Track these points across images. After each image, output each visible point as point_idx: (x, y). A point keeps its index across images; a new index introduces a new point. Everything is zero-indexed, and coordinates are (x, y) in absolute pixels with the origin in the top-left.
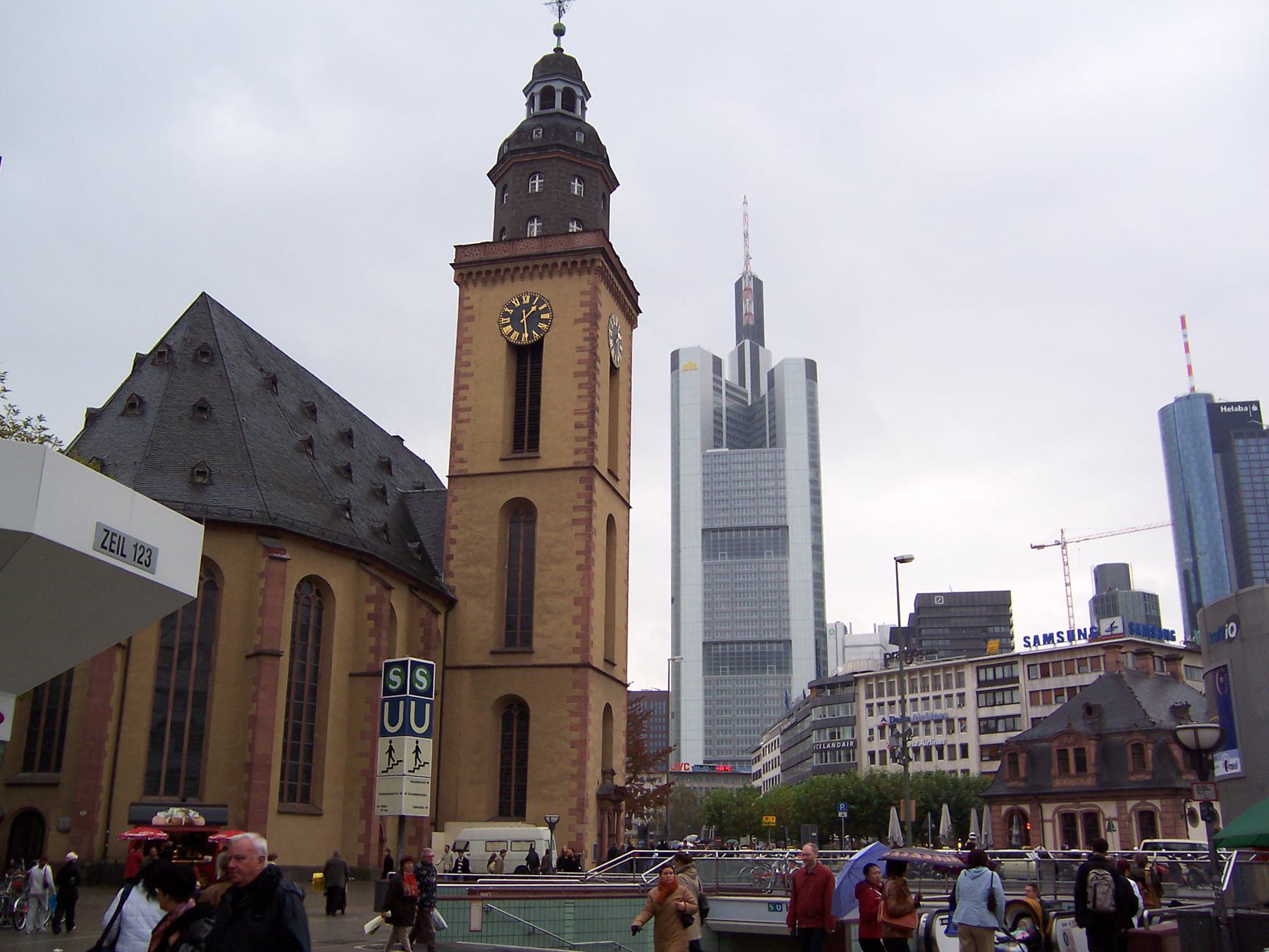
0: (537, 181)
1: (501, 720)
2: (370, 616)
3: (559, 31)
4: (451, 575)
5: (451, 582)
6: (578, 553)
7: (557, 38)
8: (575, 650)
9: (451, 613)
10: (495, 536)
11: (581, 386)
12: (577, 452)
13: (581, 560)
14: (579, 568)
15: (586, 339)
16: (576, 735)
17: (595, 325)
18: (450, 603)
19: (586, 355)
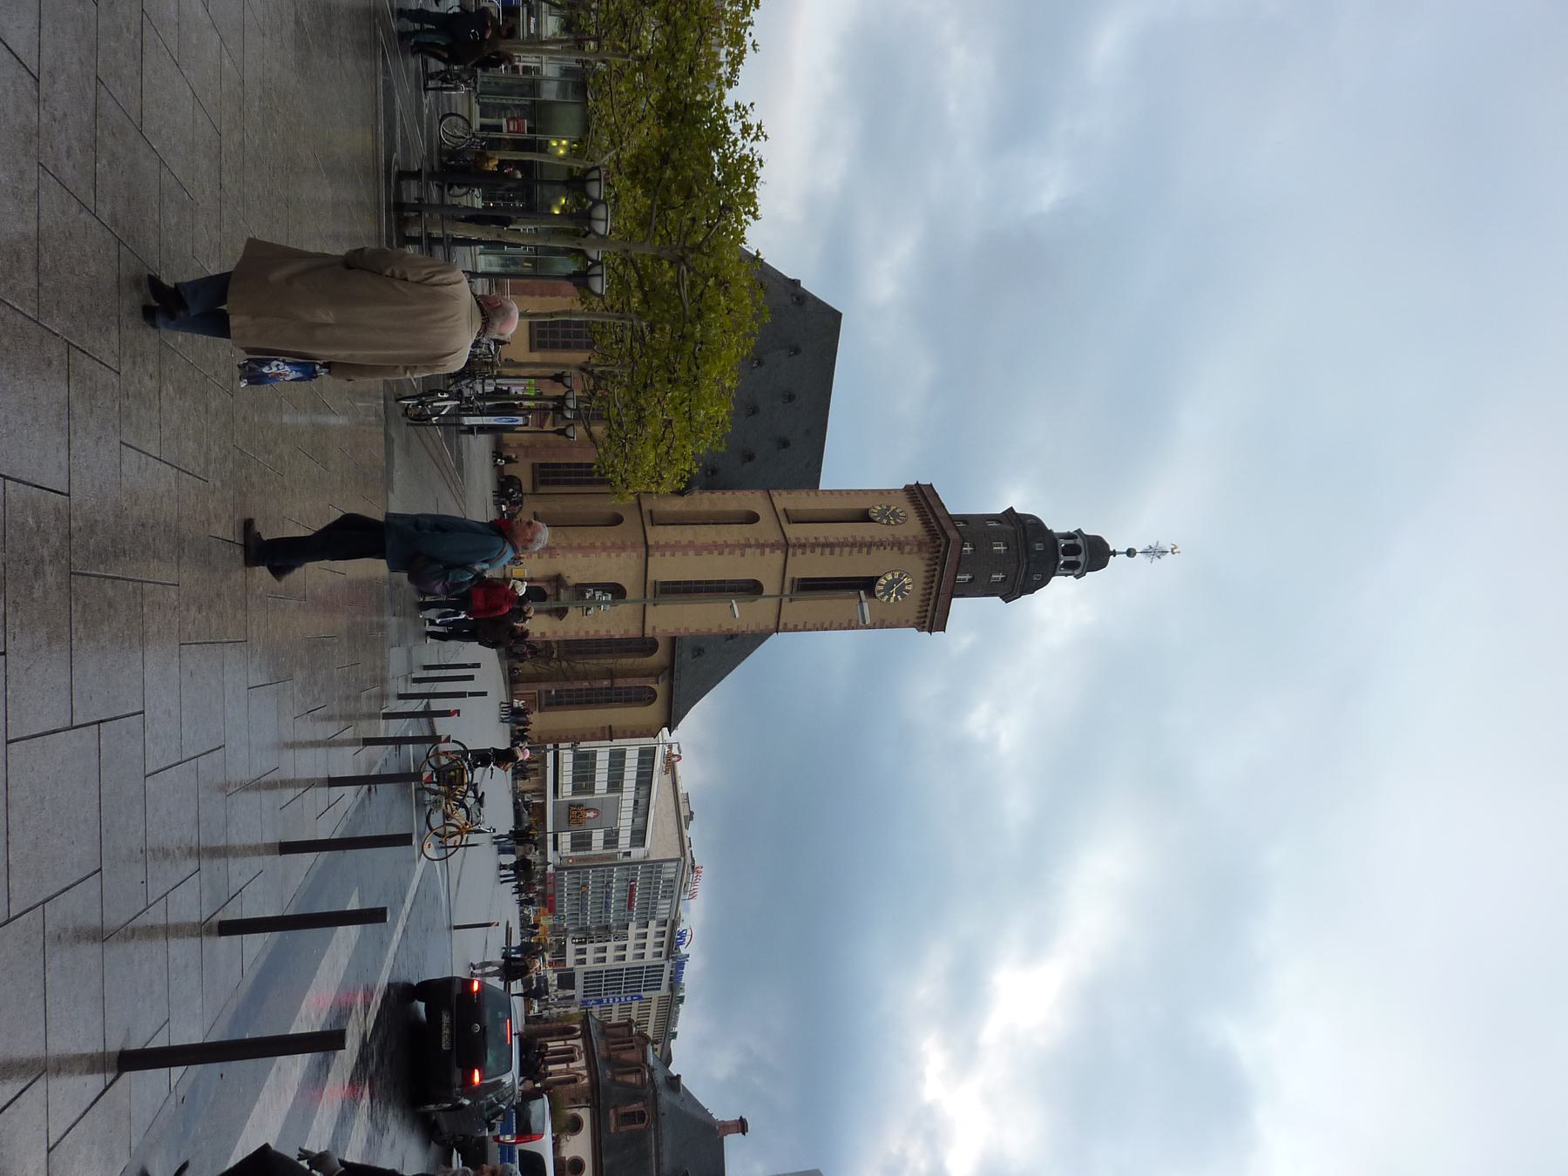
3: (1131, 553)
7: (1125, 551)
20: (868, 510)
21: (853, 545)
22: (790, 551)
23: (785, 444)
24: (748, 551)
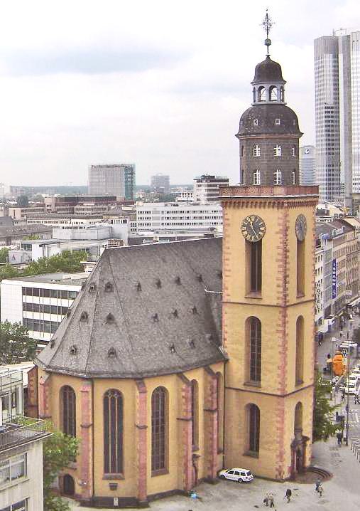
2: (183, 397)
4: (226, 347)
6: (279, 346)
10: (243, 332)
11: (279, 266)
12: (278, 298)
15: (281, 243)
16: (279, 425)
18: (226, 361)
20: (246, 240)
22: (287, 304)
24: (286, 332)
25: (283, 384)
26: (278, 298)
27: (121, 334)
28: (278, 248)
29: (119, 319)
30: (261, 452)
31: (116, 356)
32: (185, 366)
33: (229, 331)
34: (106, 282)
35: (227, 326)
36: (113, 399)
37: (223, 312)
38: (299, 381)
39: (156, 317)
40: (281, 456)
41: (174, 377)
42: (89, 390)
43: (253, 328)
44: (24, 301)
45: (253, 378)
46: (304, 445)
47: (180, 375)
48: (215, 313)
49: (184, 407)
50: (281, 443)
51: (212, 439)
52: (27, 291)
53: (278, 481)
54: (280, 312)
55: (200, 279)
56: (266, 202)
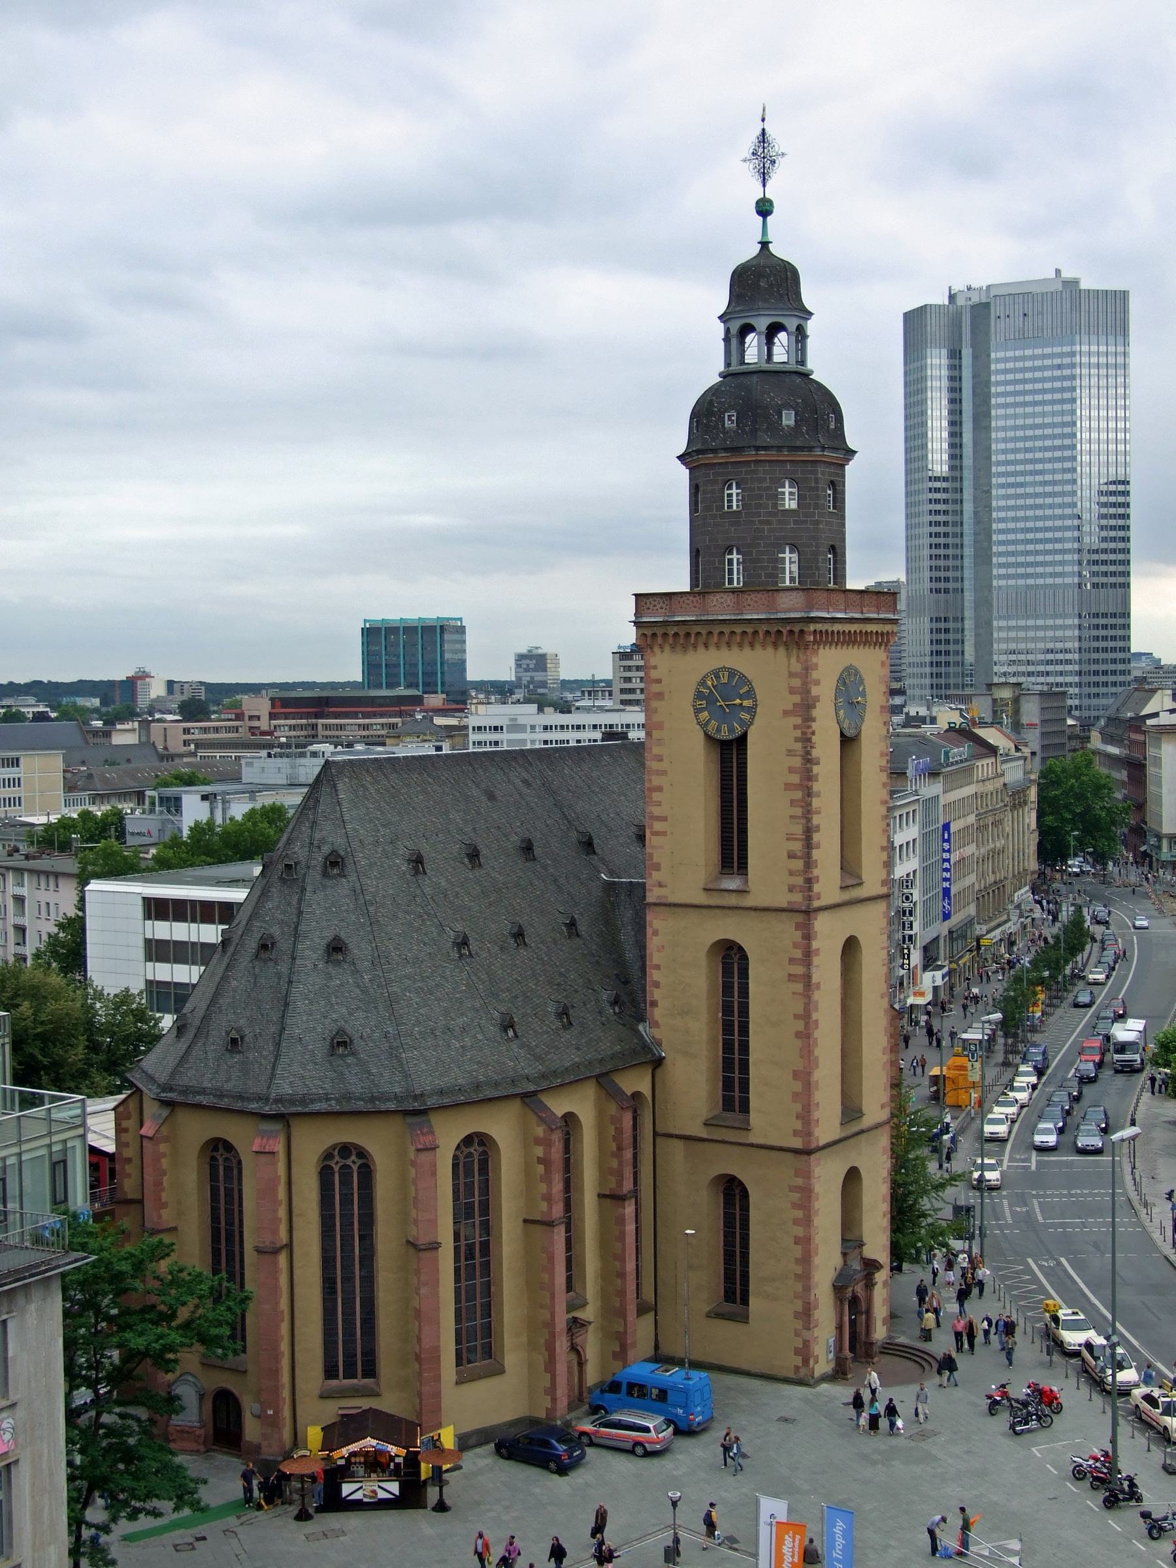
0: (734, 491)
1: (722, 1196)
2: (540, 1161)
3: (764, 209)
4: (656, 1024)
5: (656, 1033)
6: (796, 1017)
8: (796, 1133)
9: (659, 1072)
11: (793, 803)
12: (791, 889)
13: (800, 1026)
14: (798, 1035)
15: (797, 740)
16: (799, 1231)
17: (808, 719)
19: (797, 762)
20: (708, 737)
21: (809, 793)
22: (816, 904)
23: (527, 848)
24: (814, 980)
25: (806, 1116)
26: (791, 889)
27: (364, 991)
28: (790, 753)
29: (360, 949)
30: (755, 1303)
31: (354, 1054)
32: (544, 1076)
33: (662, 981)
34: (326, 849)
35: (658, 967)
36: (346, 1171)
37: (649, 931)
38: (851, 1111)
39: (462, 942)
40: (806, 1314)
41: (515, 1106)
42: (280, 1148)
43: (727, 971)
44: (149, 936)
45: (728, 1104)
46: (870, 1284)
47: (528, 1098)
48: (626, 936)
49: (543, 1188)
50: (805, 1278)
51: (622, 1275)
52: (157, 909)
53: (800, 1382)
54: (798, 927)
55: (588, 845)
56: (756, 633)
